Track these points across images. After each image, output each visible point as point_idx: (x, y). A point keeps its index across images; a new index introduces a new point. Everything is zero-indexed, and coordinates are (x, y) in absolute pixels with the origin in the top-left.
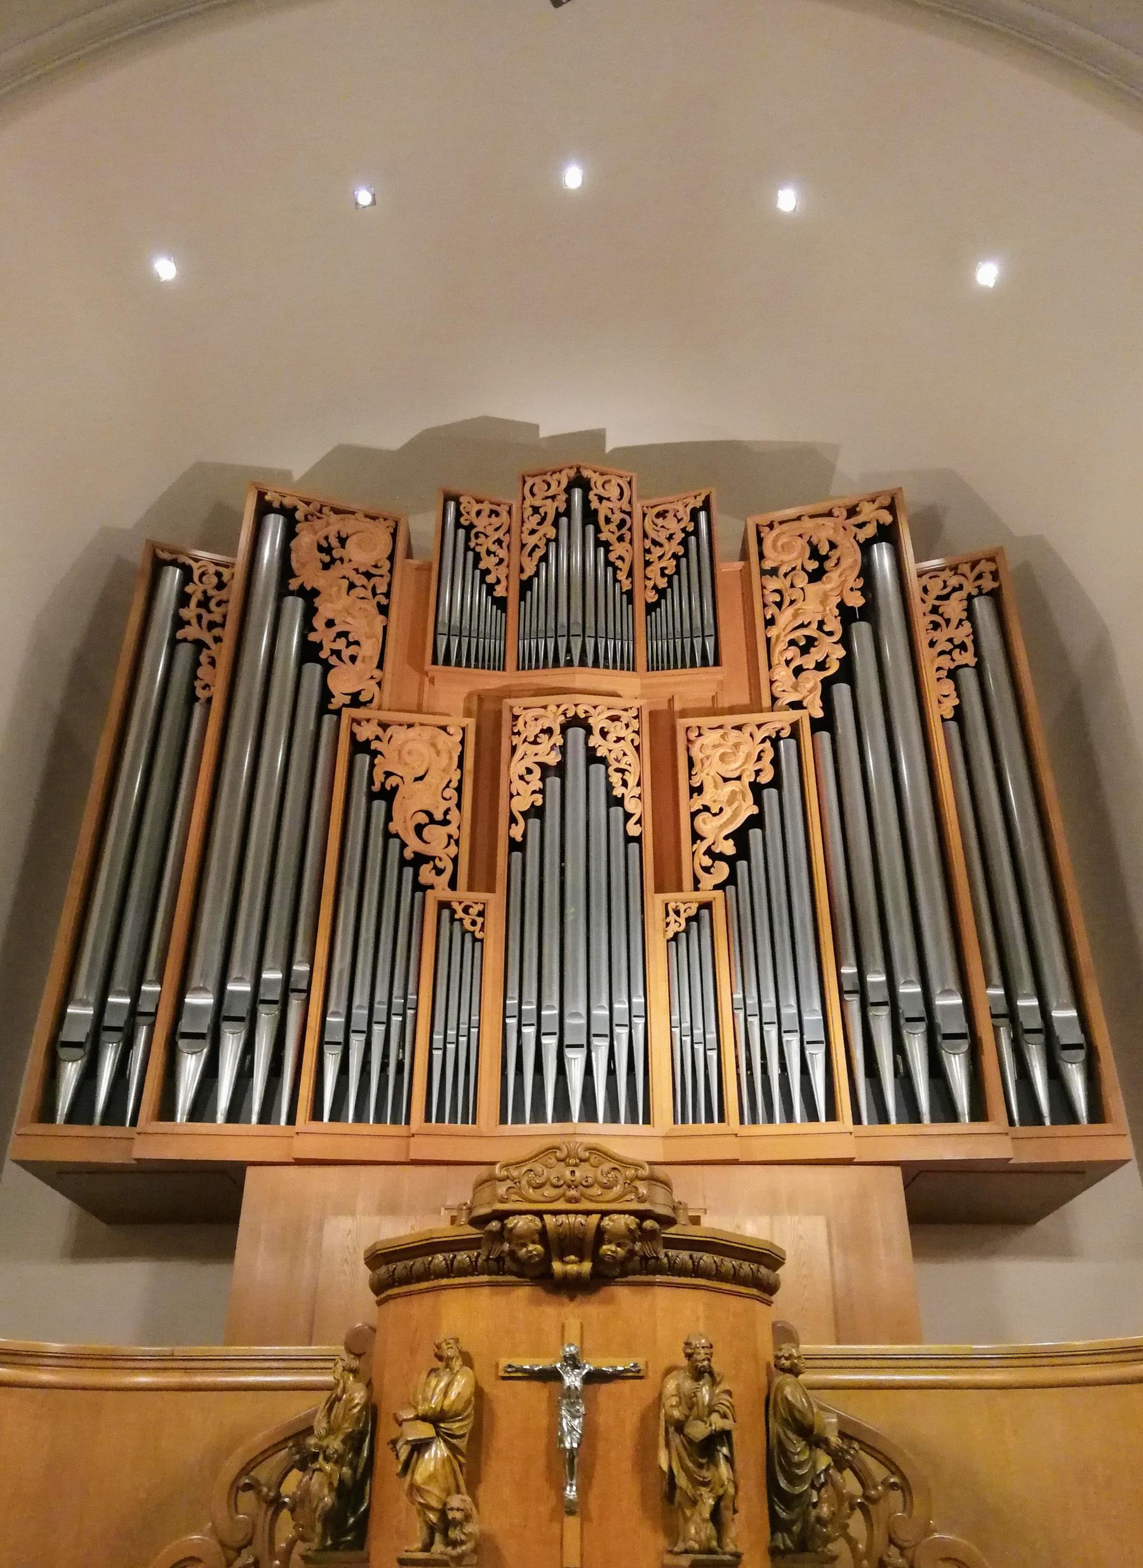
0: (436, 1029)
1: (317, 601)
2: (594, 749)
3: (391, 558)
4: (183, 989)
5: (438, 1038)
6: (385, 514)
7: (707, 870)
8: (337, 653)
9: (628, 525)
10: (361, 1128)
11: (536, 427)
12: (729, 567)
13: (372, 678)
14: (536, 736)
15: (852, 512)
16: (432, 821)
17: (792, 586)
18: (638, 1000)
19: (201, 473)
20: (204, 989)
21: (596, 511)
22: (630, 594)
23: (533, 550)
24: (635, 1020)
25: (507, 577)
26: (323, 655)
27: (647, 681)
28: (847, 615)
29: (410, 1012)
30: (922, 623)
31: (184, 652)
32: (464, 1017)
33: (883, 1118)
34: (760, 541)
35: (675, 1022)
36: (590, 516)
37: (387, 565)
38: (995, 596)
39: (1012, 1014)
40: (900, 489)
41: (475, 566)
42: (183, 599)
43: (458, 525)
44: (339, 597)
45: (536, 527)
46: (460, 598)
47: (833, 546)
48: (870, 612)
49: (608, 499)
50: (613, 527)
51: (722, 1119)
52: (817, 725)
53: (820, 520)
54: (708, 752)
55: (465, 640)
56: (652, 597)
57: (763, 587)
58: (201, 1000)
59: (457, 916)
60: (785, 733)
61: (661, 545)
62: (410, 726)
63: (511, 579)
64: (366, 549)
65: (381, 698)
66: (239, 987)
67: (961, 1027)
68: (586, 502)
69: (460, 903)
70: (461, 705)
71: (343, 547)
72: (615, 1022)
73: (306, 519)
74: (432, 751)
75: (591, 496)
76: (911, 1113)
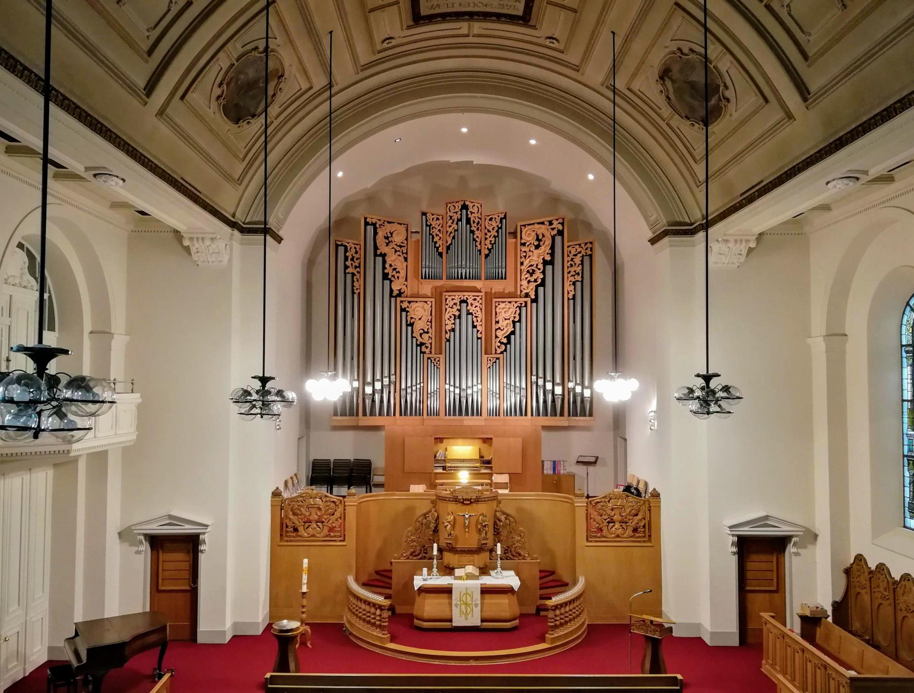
3: (407, 239)
8: (393, 276)
15: (551, 223)
22: (480, 251)
28: (545, 263)
31: (349, 277)
33: (539, 415)
36: (468, 221)
38: (591, 256)
42: (346, 258)
43: (427, 225)
47: (543, 236)
52: (533, 301)
64: (398, 238)
68: (467, 215)
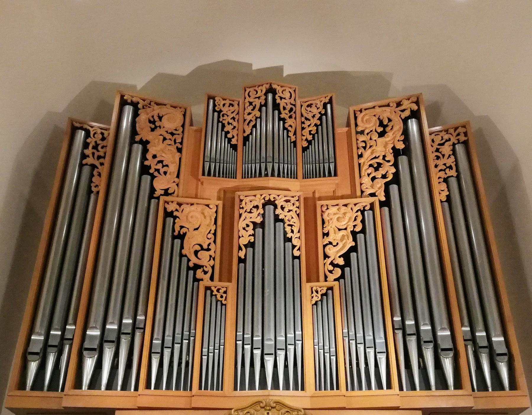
0: (204, 346)
1: (148, 146)
2: (278, 215)
3: (183, 126)
4: (85, 328)
5: (205, 350)
6: (180, 105)
7: (331, 272)
8: (158, 170)
9: (294, 111)
10: (169, 392)
11: (251, 65)
12: (341, 130)
13: (174, 182)
14: (251, 209)
15: (399, 104)
16: (202, 249)
17: (371, 139)
18: (298, 333)
19: (95, 86)
20: (95, 328)
21: (279, 104)
22: (295, 143)
23: (249, 122)
24: (297, 342)
25: (237, 135)
26: (151, 171)
27: (303, 184)
28: (396, 152)
29: (192, 338)
30: (431, 156)
31: (86, 170)
32: (217, 341)
34: (356, 118)
35: (316, 343)
36: (276, 106)
37: (181, 129)
38: (466, 144)
39: (473, 339)
40: (421, 94)
41: (222, 130)
42: (86, 145)
43: (214, 111)
44: (158, 144)
45: (251, 112)
46: (215, 145)
47: (390, 120)
48: (407, 151)
49: (285, 98)
50: (287, 111)
51: (338, 388)
52: (382, 204)
53: (384, 108)
54: (331, 217)
55: (218, 164)
56: (305, 144)
57: (357, 140)
58: (94, 332)
59: (214, 294)
60: (368, 208)
61: (309, 120)
62: (192, 204)
63: (239, 136)
65: (178, 192)
66: (112, 326)
67: (449, 345)
68: (274, 100)
69: (215, 287)
70: (216, 194)
71: (161, 121)
72: (288, 343)
73: (143, 108)
74: (202, 216)
75: (277, 97)
76: (426, 385)
